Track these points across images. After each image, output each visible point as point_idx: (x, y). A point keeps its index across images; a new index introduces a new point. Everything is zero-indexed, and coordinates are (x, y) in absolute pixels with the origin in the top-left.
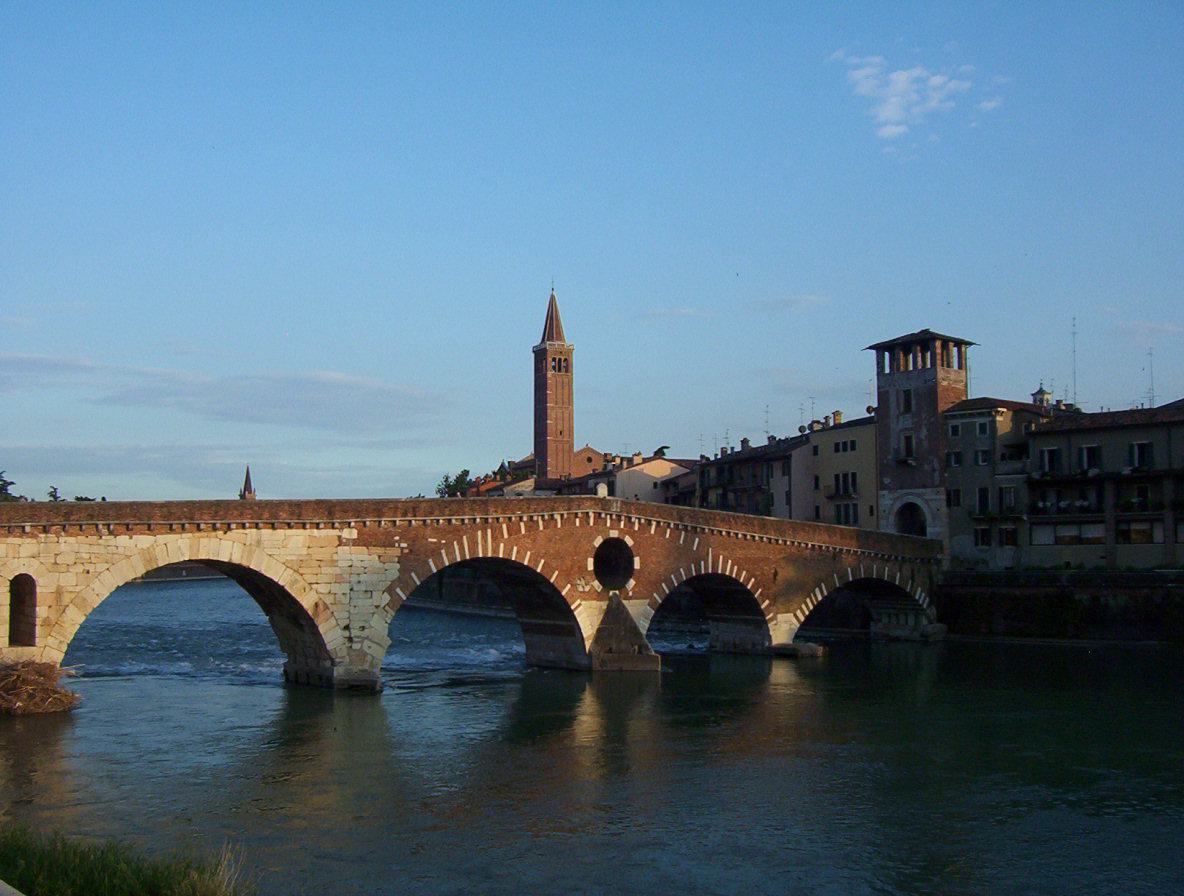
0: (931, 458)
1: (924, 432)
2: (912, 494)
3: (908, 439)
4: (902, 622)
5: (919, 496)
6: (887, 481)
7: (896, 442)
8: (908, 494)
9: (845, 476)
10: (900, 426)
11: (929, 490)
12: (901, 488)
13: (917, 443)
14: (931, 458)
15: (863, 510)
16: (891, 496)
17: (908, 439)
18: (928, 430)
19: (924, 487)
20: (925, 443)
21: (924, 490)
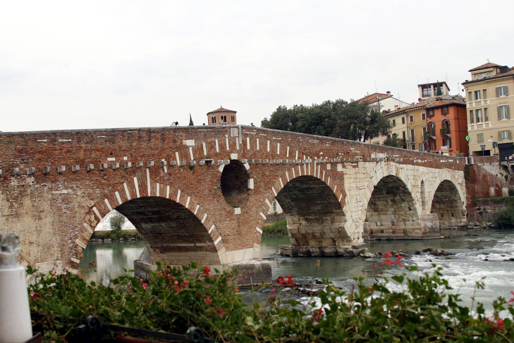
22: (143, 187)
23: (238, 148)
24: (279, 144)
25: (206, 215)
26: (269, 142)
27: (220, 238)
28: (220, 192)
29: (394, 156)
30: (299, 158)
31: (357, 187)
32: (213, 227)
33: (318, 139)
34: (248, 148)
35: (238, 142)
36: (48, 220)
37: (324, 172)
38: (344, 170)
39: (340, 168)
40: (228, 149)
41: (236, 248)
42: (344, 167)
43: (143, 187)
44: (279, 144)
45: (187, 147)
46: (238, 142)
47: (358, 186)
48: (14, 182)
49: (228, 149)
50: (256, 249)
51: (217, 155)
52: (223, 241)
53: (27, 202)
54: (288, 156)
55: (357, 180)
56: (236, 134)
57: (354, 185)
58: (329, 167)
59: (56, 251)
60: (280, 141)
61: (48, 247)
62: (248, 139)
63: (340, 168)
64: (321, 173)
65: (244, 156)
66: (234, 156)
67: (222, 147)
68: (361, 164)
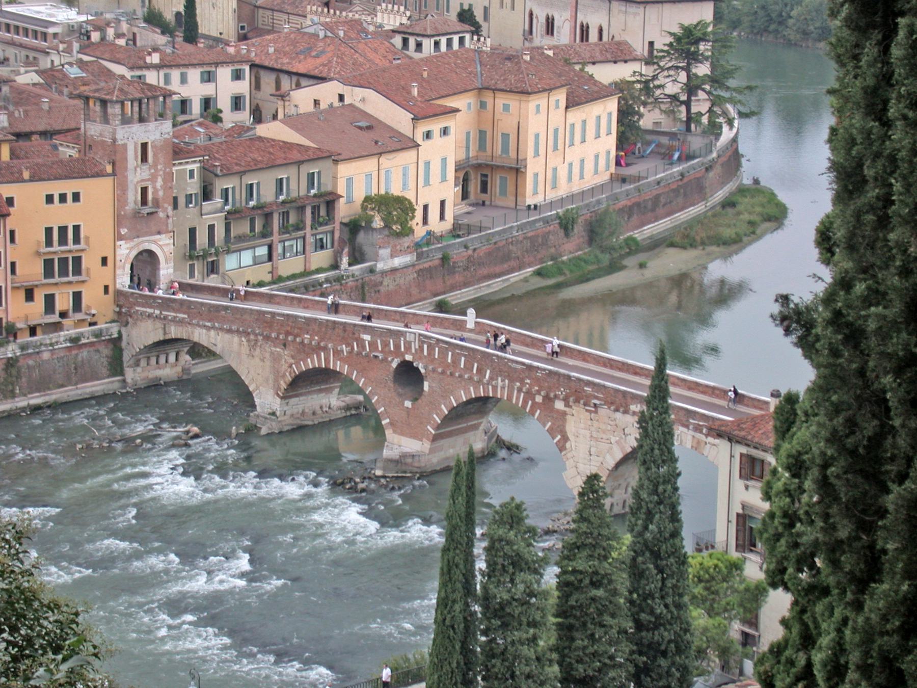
0: (166, 205)
1: (159, 183)
2: (148, 241)
3: (144, 190)
4: (162, 359)
5: (155, 242)
6: (124, 231)
7: (133, 197)
8: (143, 242)
9: (63, 230)
10: (138, 178)
11: (164, 236)
12: (138, 237)
13: (153, 193)
14: (166, 205)
15: (90, 262)
16: (128, 245)
17: (144, 190)
18: (163, 180)
19: (159, 233)
20: (161, 193)
21: (158, 237)
22: (327, 360)
23: (413, 351)
24: (463, 359)
25: (376, 398)
26: (450, 353)
27: (388, 420)
28: (392, 385)
29: (691, 421)
30: (491, 378)
31: (592, 436)
32: (382, 409)
33: (523, 364)
34: (425, 353)
35: (415, 346)
36: (268, 363)
37: (530, 402)
38: (567, 409)
39: (559, 405)
40: (403, 349)
41: (402, 434)
42: (567, 405)
43: (327, 360)
44: (463, 359)
45: (364, 341)
46: (415, 346)
47: (595, 435)
48: (252, 337)
49: (403, 349)
50: (425, 445)
51: (391, 352)
52: (391, 424)
53: (258, 350)
54: (475, 371)
55: (593, 429)
56: (412, 339)
57: (587, 433)
58: (539, 399)
59: (271, 382)
60: (465, 356)
61: (267, 380)
62: (425, 346)
63: (559, 405)
64: (525, 402)
65: (420, 358)
66: (408, 358)
67: (397, 346)
68: (604, 411)
